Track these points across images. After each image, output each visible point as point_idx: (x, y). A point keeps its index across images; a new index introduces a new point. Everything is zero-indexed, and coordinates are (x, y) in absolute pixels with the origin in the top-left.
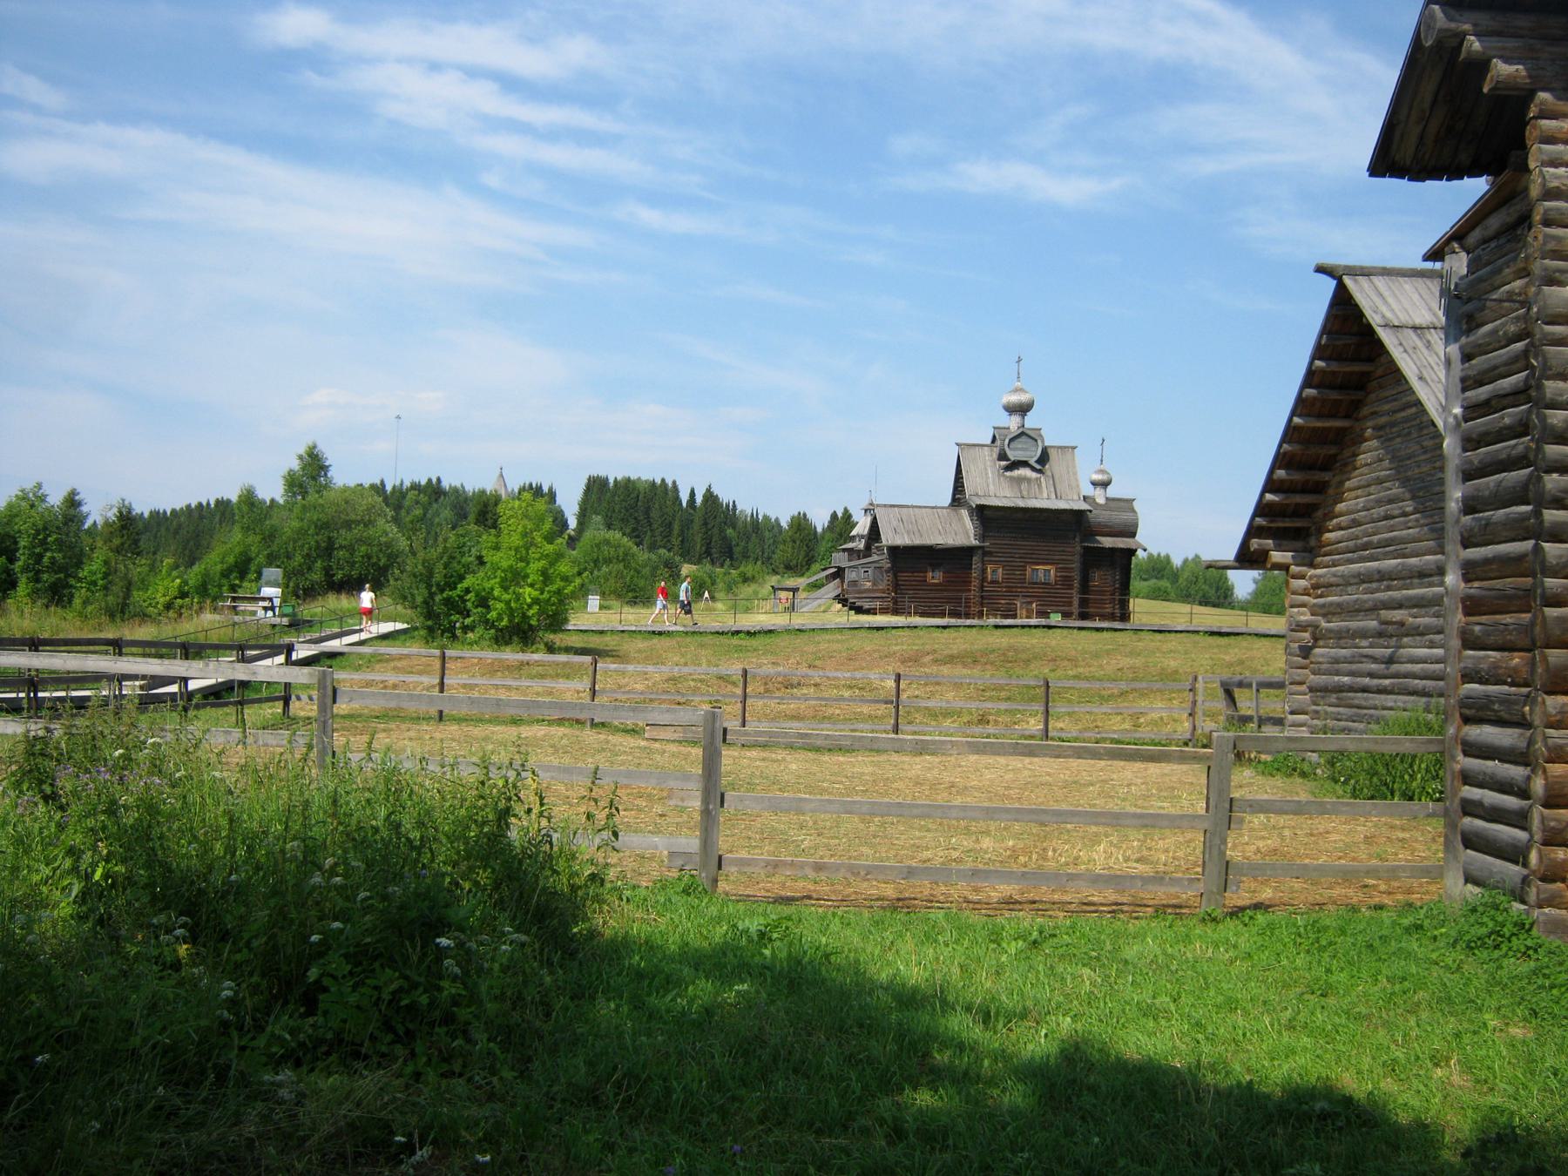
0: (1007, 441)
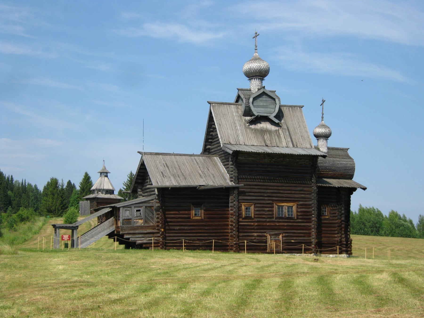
0: (251, 100)
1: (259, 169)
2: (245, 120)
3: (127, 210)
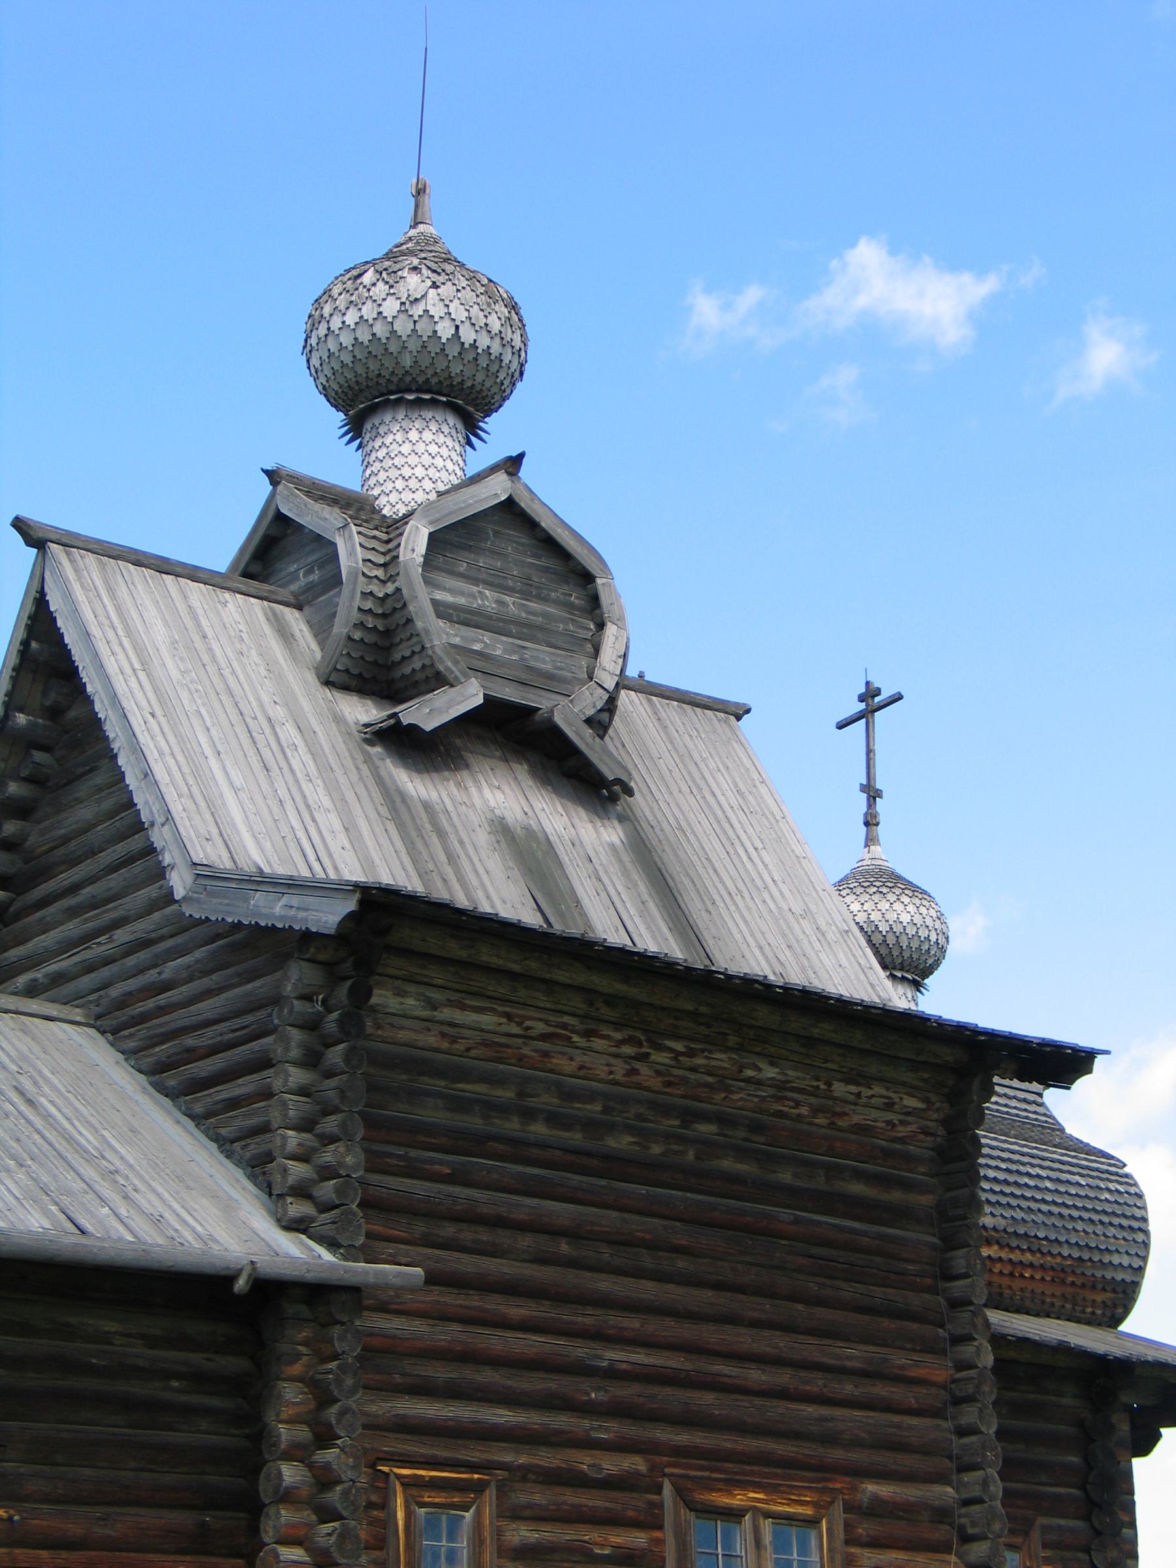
1: (539, 1129)
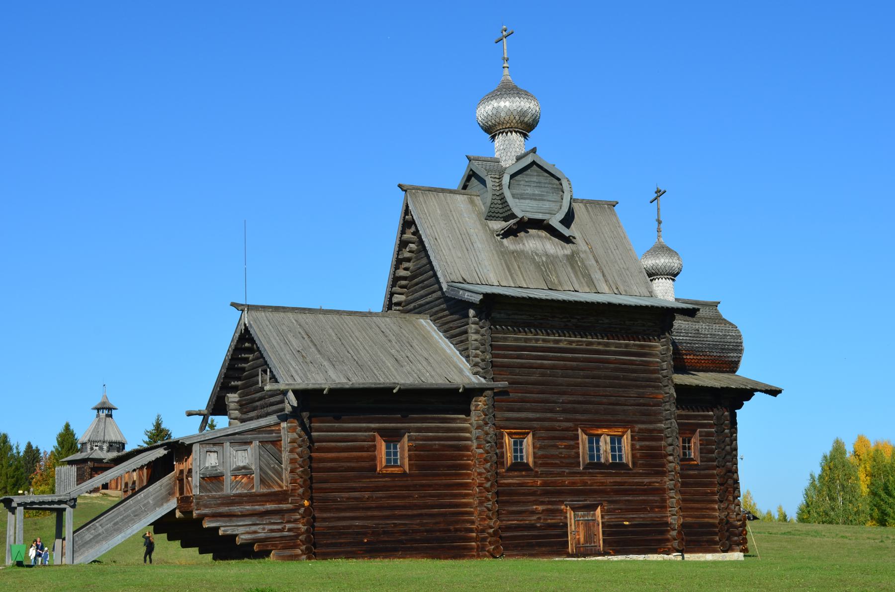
0: (506, 179)
2: (492, 231)
3: (211, 452)
